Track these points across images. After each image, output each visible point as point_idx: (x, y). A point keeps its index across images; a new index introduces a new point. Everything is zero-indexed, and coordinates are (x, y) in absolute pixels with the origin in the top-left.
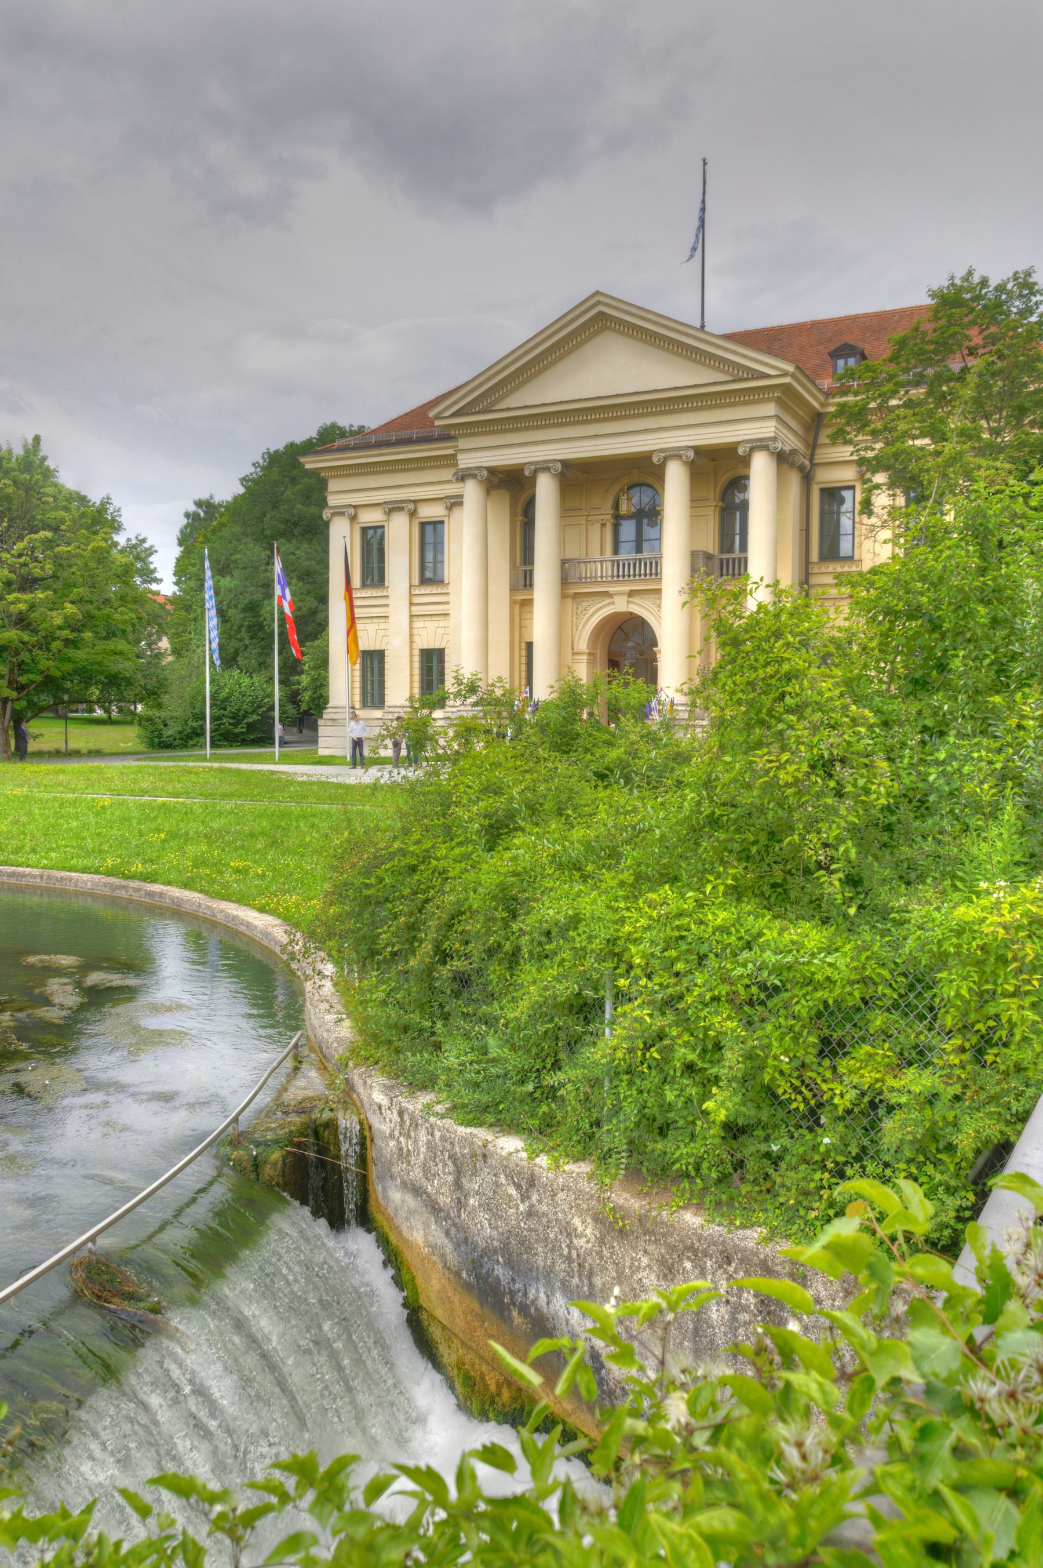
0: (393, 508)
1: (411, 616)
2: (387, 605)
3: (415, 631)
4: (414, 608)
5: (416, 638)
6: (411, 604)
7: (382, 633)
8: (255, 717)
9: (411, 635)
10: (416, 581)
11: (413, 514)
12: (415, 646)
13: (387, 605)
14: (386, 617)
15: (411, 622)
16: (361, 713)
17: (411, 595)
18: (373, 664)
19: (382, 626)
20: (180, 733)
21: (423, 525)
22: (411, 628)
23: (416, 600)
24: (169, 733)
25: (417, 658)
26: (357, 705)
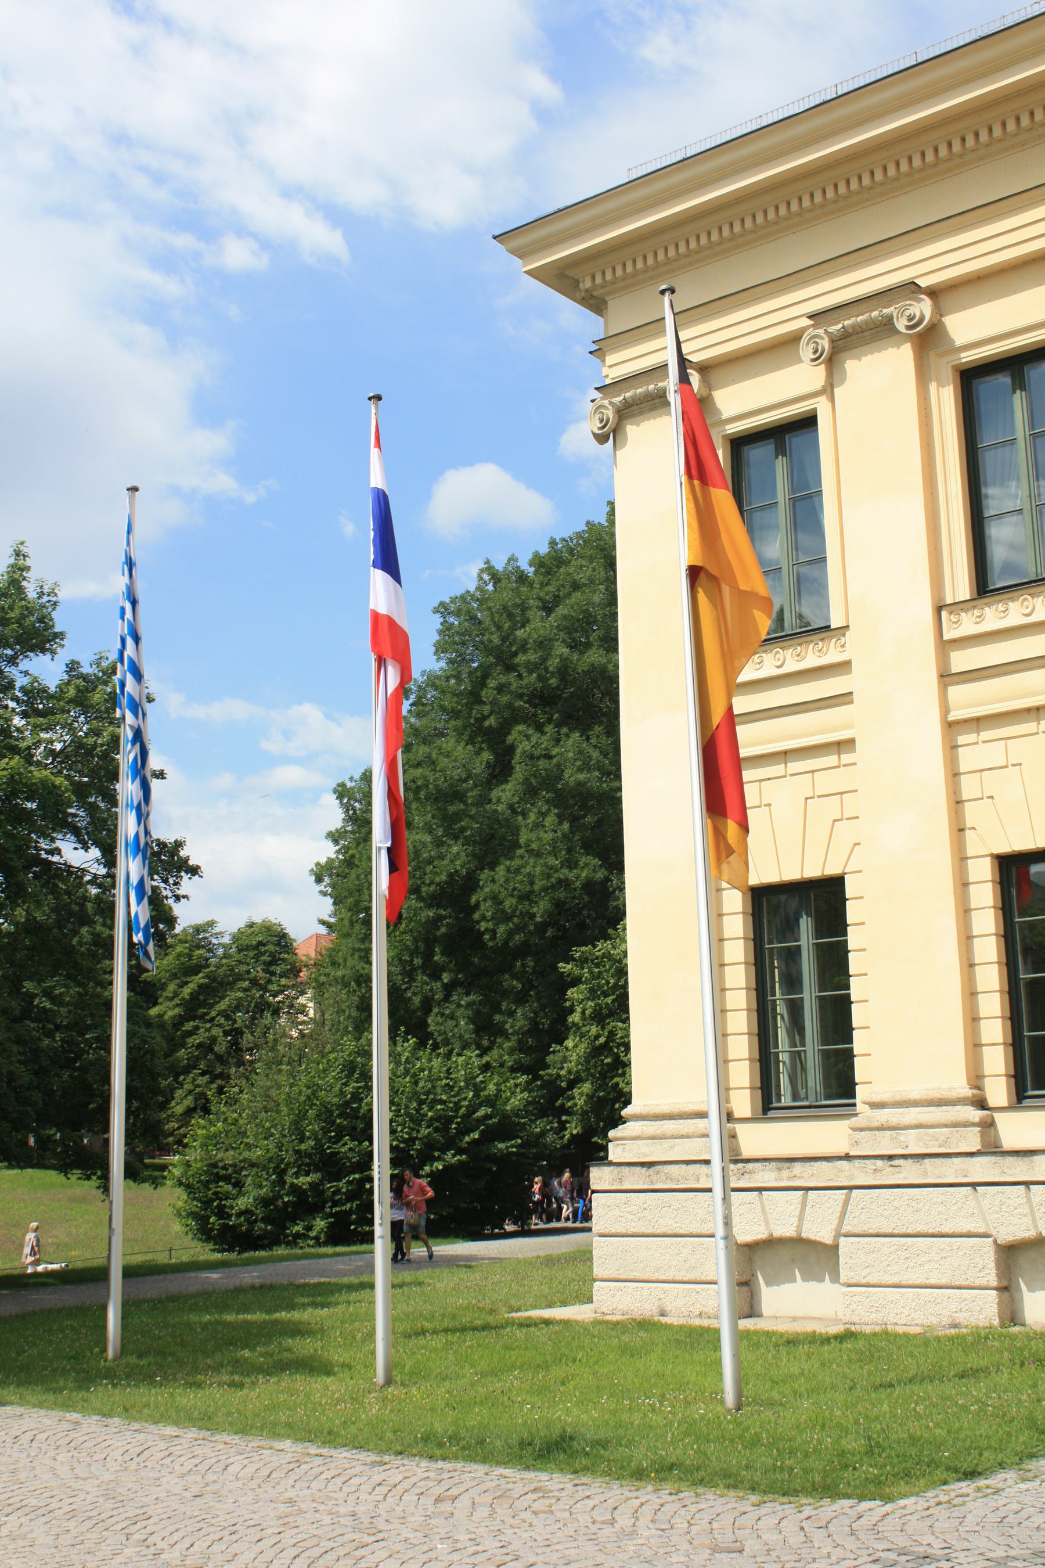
0: (849, 335)
1: (952, 727)
2: (844, 698)
3: (969, 787)
4: (957, 693)
5: (971, 813)
6: (947, 678)
7: (832, 807)
8: (451, 1158)
9: (957, 803)
10: (960, 583)
11: (928, 339)
12: (974, 844)
13: (844, 698)
14: (849, 744)
15: (952, 749)
16: (761, 1138)
17: (945, 646)
18: (799, 932)
19: (826, 782)
20: (265, 1202)
21: (970, 378)
22: (954, 775)
23: (962, 660)
24: (243, 1203)
25: (985, 895)
26: (743, 1103)
